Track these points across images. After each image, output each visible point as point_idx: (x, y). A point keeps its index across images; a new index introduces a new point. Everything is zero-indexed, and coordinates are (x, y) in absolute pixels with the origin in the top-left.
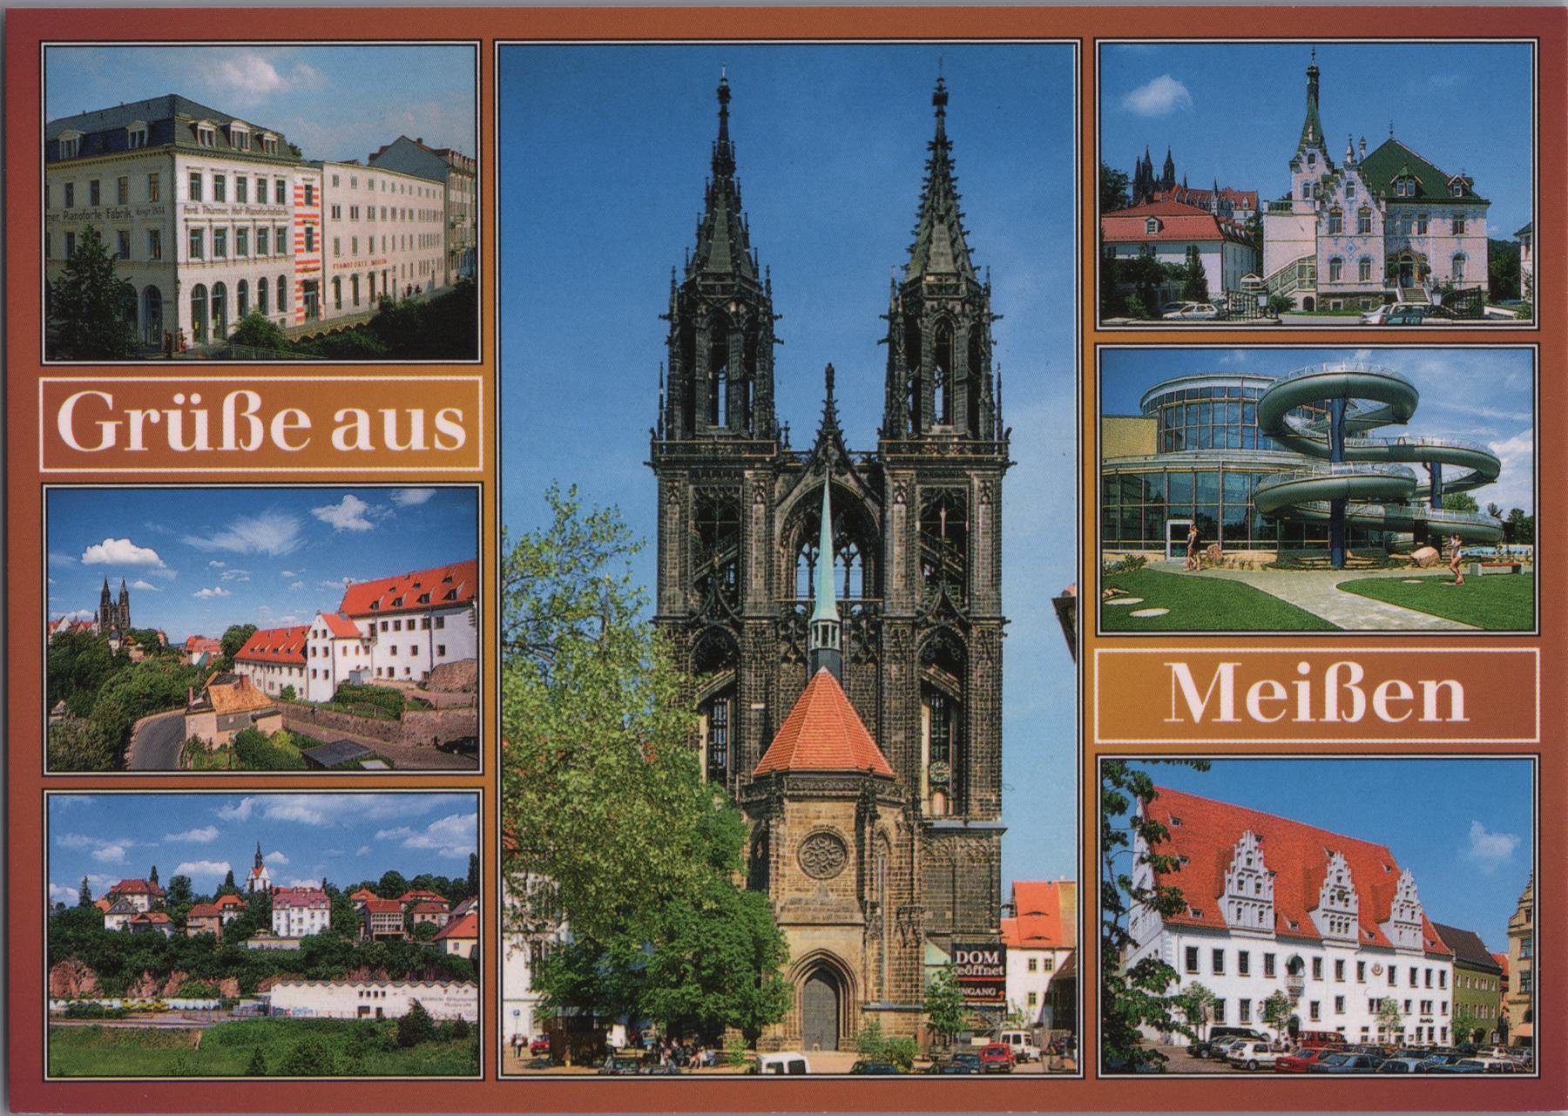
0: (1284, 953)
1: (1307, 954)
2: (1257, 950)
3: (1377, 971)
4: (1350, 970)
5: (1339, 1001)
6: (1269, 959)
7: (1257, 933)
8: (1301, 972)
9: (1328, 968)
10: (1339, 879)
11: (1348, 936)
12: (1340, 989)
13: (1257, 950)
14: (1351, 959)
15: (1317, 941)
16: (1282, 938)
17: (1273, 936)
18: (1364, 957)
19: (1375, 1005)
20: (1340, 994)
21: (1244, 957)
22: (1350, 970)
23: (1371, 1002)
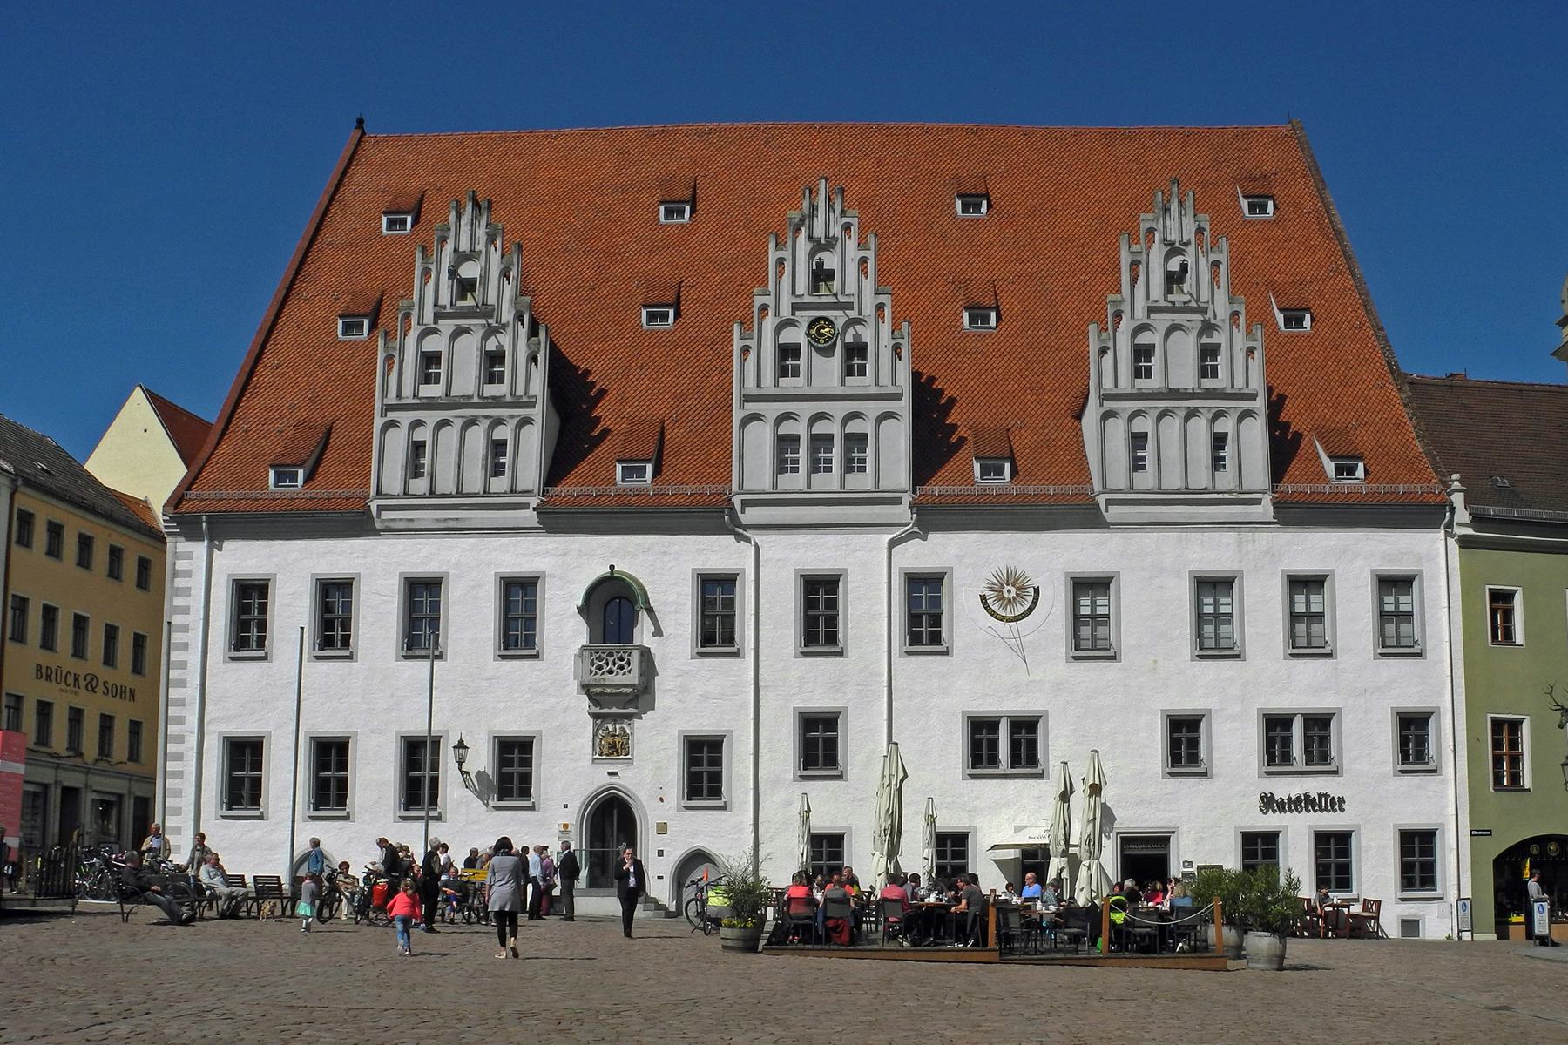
0: (569, 566)
1: (667, 567)
3: (1010, 598)
4: (870, 611)
5: (819, 742)
6: (519, 600)
8: (643, 633)
9: (771, 612)
10: (821, 276)
13: (471, 569)
16: (558, 519)
17: (529, 517)
20: (820, 703)
21: (422, 600)
22: (870, 611)
23: (981, 730)
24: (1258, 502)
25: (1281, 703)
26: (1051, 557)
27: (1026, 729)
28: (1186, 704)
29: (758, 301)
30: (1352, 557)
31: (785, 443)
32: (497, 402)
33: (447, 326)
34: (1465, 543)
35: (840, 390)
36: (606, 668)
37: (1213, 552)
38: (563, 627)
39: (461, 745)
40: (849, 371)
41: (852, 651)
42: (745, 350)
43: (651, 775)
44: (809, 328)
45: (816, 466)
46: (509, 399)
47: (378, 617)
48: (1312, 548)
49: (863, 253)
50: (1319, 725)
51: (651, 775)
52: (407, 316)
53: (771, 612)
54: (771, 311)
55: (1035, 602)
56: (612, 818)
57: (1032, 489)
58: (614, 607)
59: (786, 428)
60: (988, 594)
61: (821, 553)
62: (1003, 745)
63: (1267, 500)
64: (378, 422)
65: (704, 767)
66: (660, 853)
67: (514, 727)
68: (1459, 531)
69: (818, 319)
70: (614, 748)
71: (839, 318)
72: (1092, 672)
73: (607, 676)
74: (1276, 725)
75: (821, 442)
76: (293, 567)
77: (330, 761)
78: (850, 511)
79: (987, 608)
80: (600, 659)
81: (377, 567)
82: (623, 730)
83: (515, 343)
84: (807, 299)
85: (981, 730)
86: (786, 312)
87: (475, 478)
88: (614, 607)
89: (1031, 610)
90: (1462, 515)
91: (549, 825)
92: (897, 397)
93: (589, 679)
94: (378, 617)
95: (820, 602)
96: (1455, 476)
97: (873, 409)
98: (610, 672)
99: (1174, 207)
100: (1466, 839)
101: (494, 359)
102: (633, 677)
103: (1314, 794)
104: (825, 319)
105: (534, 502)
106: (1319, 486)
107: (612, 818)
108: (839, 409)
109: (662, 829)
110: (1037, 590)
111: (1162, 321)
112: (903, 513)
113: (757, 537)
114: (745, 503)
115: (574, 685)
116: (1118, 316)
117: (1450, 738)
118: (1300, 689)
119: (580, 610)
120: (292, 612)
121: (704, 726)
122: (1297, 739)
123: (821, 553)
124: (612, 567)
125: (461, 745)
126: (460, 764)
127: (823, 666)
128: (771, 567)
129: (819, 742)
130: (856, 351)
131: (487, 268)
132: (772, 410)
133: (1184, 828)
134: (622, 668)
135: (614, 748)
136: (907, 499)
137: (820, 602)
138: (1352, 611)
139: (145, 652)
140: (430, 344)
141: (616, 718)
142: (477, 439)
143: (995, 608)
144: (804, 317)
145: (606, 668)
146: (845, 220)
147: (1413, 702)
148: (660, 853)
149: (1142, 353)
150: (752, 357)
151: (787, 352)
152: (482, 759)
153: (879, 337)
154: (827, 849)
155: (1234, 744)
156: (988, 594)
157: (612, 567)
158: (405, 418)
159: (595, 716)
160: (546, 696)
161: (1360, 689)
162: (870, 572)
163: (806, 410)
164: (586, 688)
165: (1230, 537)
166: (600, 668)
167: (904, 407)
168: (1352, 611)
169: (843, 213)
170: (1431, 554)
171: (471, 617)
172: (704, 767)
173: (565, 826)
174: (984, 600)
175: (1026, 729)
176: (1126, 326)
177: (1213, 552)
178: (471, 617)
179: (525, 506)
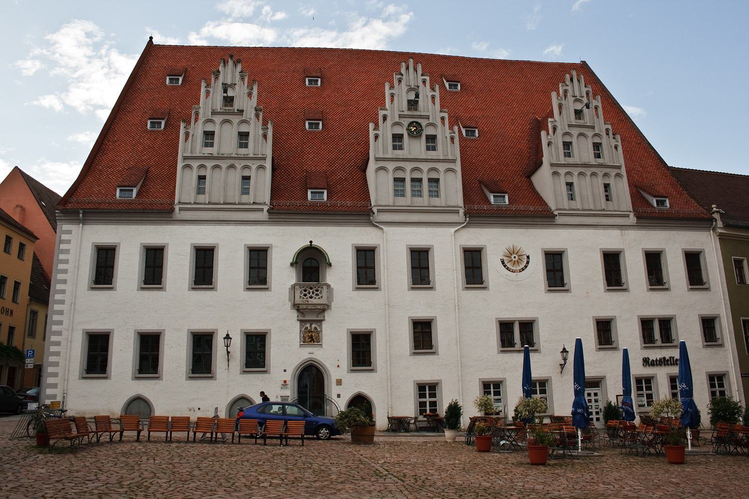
0: (286, 242)
1: (339, 242)
2: (231, 244)
3: (515, 260)
4: (447, 267)
5: (423, 334)
7: (226, 212)
9: (394, 267)
10: (413, 104)
11: (436, 201)
12: (421, 305)
14: (446, 246)
15: (359, 210)
17: (264, 216)
18: (475, 237)
19: (517, 335)
20: (422, 314)
22: (447, 267)
23: (505, 327)
24: (628, 216)
25: (649, 312)
26: (535, 241)
27: (527, 327)
28: (604, 314)
29: (381, 113)
30: (673, 244)
31: (399, 181)
32: (246, 158)
33: (218, 119)
34: (722, 238)
35: (423, 156)
36: (308, 296)
37: (611, 240)
38: (283, 274)
39: (228, 337)
40: (428, 149)
41: (438, 286)
42: (376, 137)
43: (333, 353)
44: (409, 126)
45: (417, 193)
46: (251, 155)
47: (179, 267)
48: (654, 239)
49: (434, 93)
50: (666, 324)
51: (333, 353)
52: (197, 114)
53: (394, 267)
54: (389, 119)
55: (528, 263)
56: (311, 379)
57: (522, 207)
58: (311, 264)
59: (400, 175)
60: (505, 258)
61: (420, 237)
62: (517, 335)
63: (632, 215)
64: (180, 165)
65: (361, 349)
66: (339, 396)
67: (256, 326)
68: (720, 231)
69: (412, 122)
70: (311, 337)
71: (423, 122)
72: (558, 298)
73: (310, 299)
74: (646, 324)
75: (417, 181)
76: (130, 240)
77: (149, 348)
78: (434, 216)
79: (505, 266)
80: (305, 291)
81: (179, 242)
82: (315, 328)
83: (254, 129)
84: (406, 113)
85: (505, 327)
86: (397, 119)
87: (234, 195)
88: (311, 264)
89: (526, 267)
90: (720, 224)
91: (276, 384)
92: (454, 161)
93: (298, 300)
94: (179, 267)
95: (420, 264)
96: (713, 206)
97: (442, 167)
98: (311, 297)
99: (575, 80)
100: (740, 378)
101: (244, 136)
102: (323, 301)
103: (667, 358)
104: (417, 123)
105: (266, 208)
106: (649, 210)
107: (311, 379)
108: (425, 167)
109: (339, 382)
110: (528, 257)
111: (575, 132)
112: (460, 217)
113: (385, 228)
114: (379, 211)
115: (289, 305)
116: (555, 129)
117: (726, 328)
118: (657, 305)
119: (292, 264)
120: (129, 265)
121: (361, 326)
122: (657, 330)
123: (420, 237)
124: (311, 242)
125: (228, 337)
126: (227, 347)
127: (421, 295)
128: (394, 246)
129: (423, 334)
130: (431, 139)
131: (239, 92)
132: (391, 166)
133: (607, 377)
134: (317, 295)
135: (311, 337)
136: (462, 211)
137: (420, 264)
138: (675, 269)
139: (41, 287)
140: (209, 127)
141: (311, 322)
142: (235, 178)
143: (508, 265)
144: (406, 122)
145: (308, 296)
146: (423, 77)
147: (708, 312)
148: (339, 396)
149: (567, 145)
150: (380, 139)
151: (397, 138)
152: (238, 345)
153: (443, 133)
154: (427, 390)
155: (628, 334)
156: (505, 258)
157: (311, 242)
158: (195, 164)
159: (301, 321)
160: (272, 310)
161: (683, 305)
162: (446, 246)
163: (409, 166)
164: (296, 307)
165: (616, 233)
166: (305, 295)
167: (458, 167)
168: (675, 269)
169: (422, 75)
170: (708, 243)
171: (231, 267)
172: (361, 349)
173: (285, 382)
174: (503, 262)
175: (527, 327)
176: (559, 132)
177: (611, 240)
178: (231, 267)
179: (262, 210)
